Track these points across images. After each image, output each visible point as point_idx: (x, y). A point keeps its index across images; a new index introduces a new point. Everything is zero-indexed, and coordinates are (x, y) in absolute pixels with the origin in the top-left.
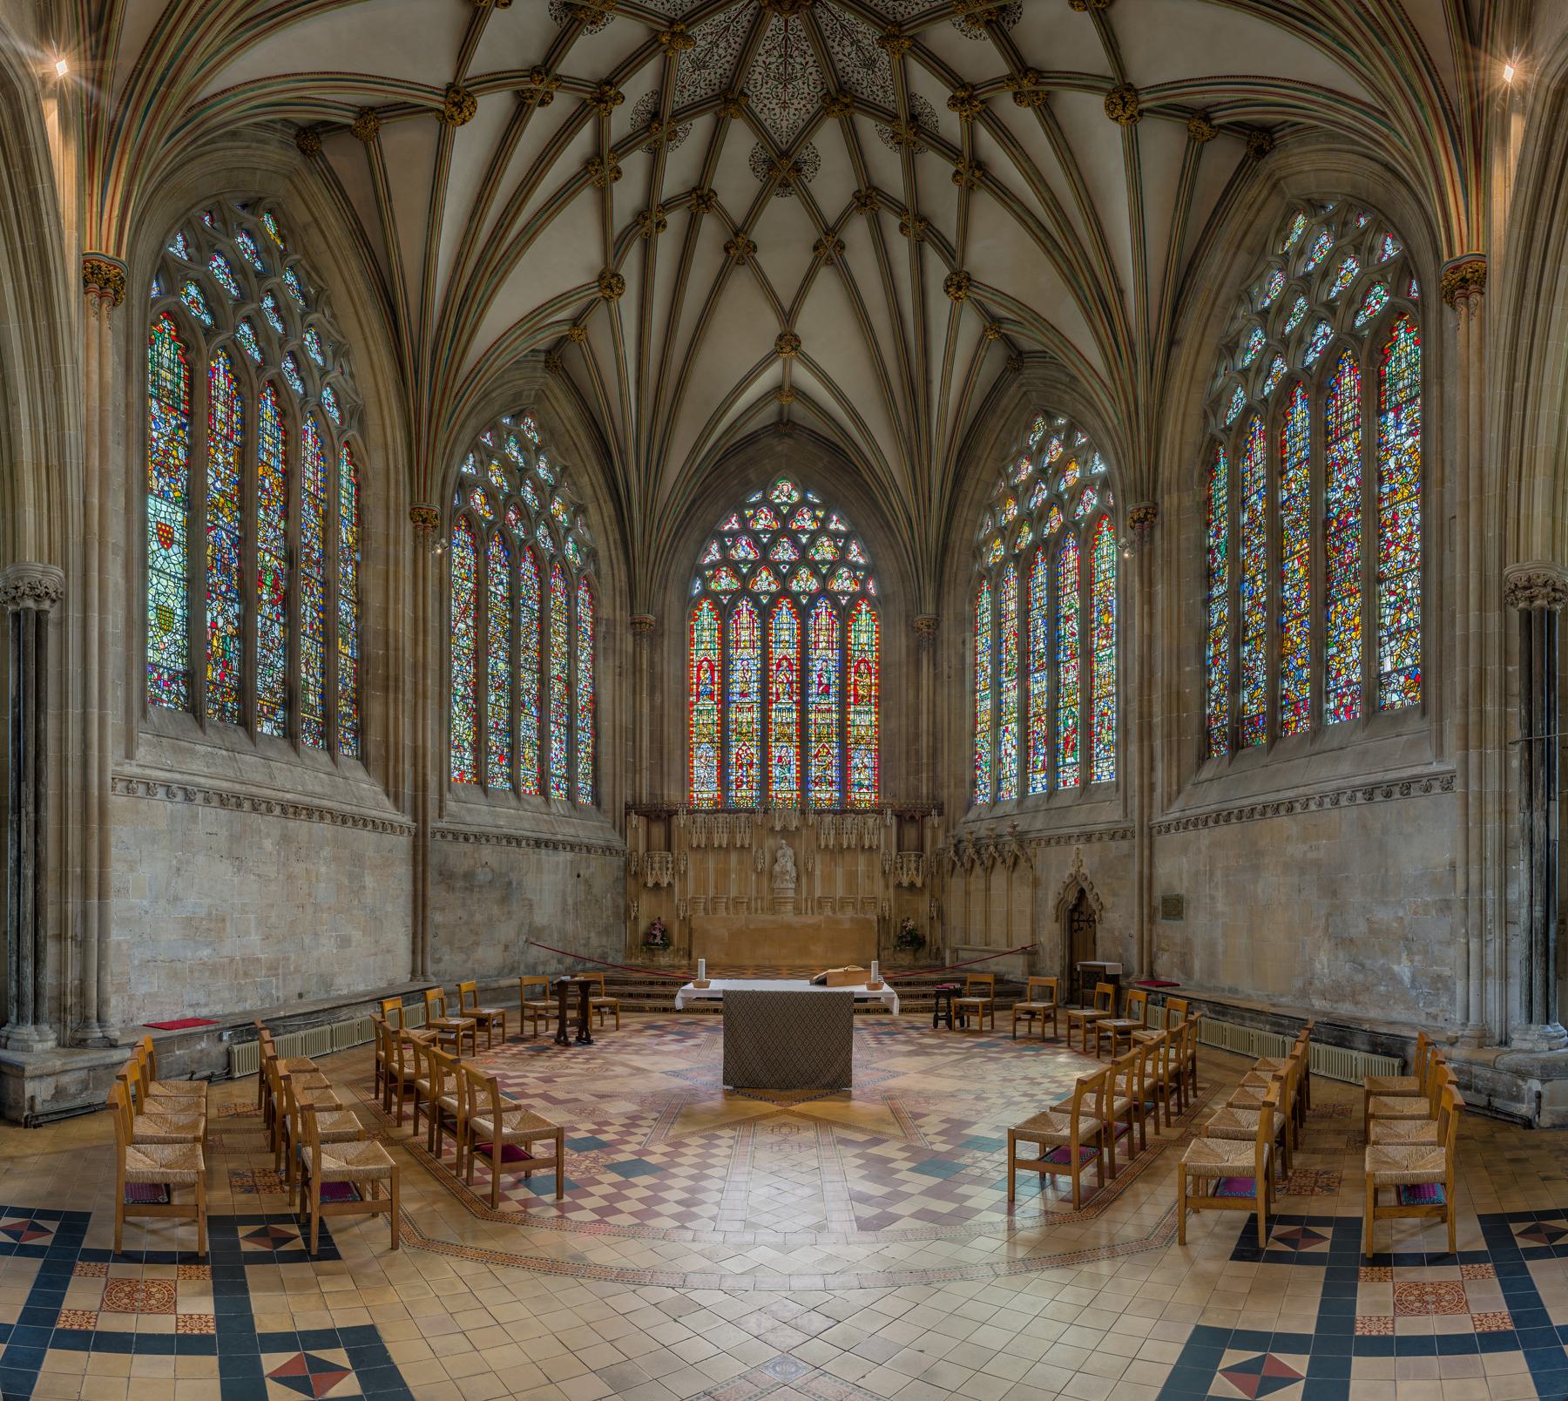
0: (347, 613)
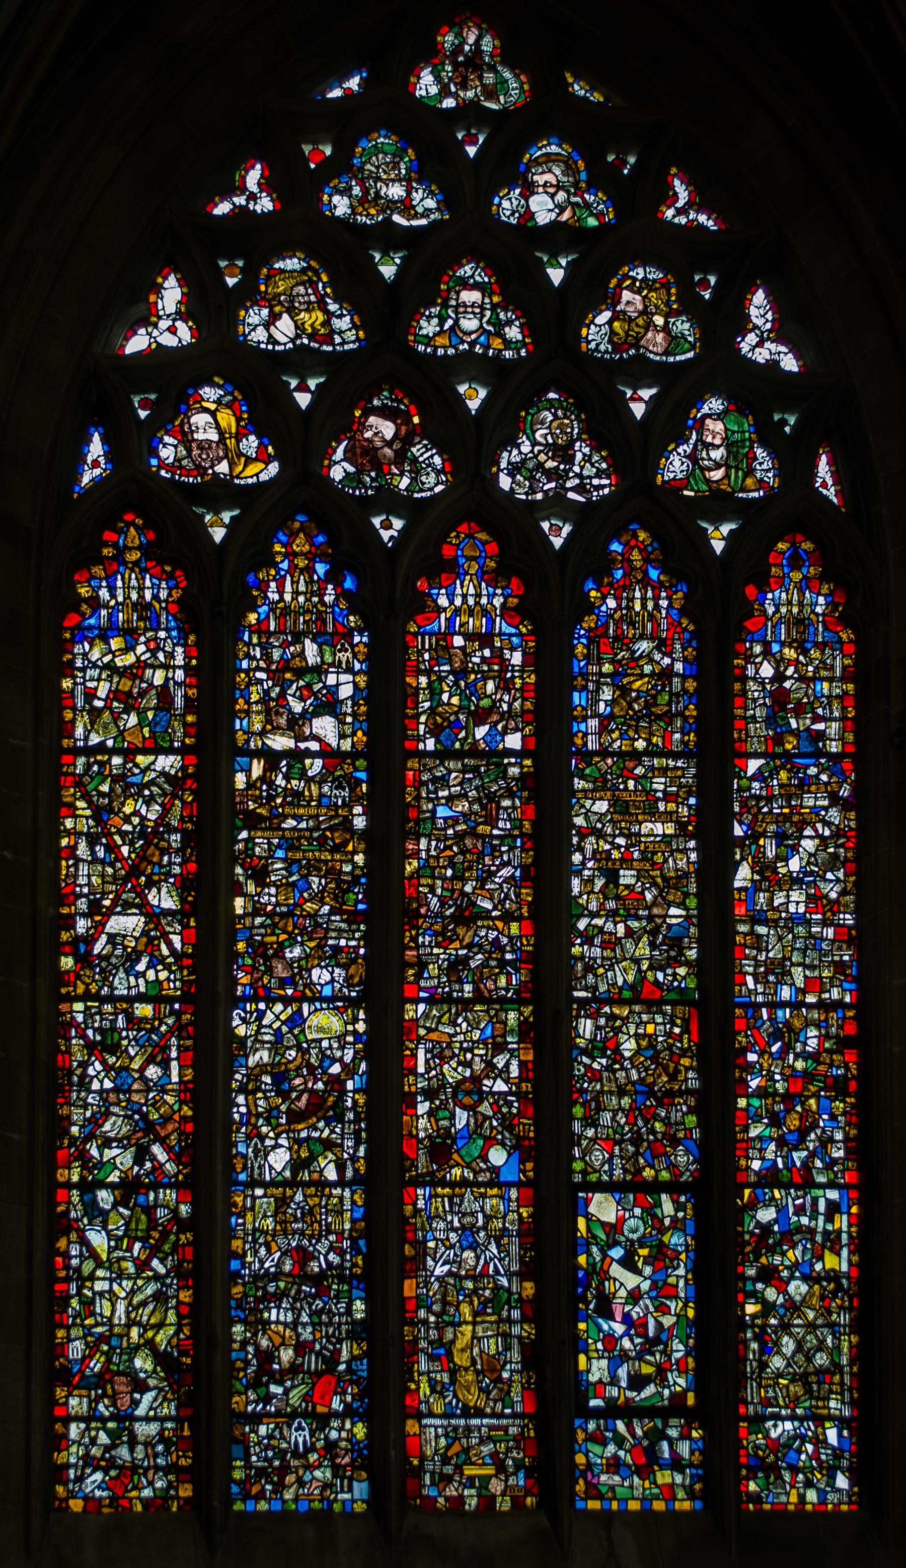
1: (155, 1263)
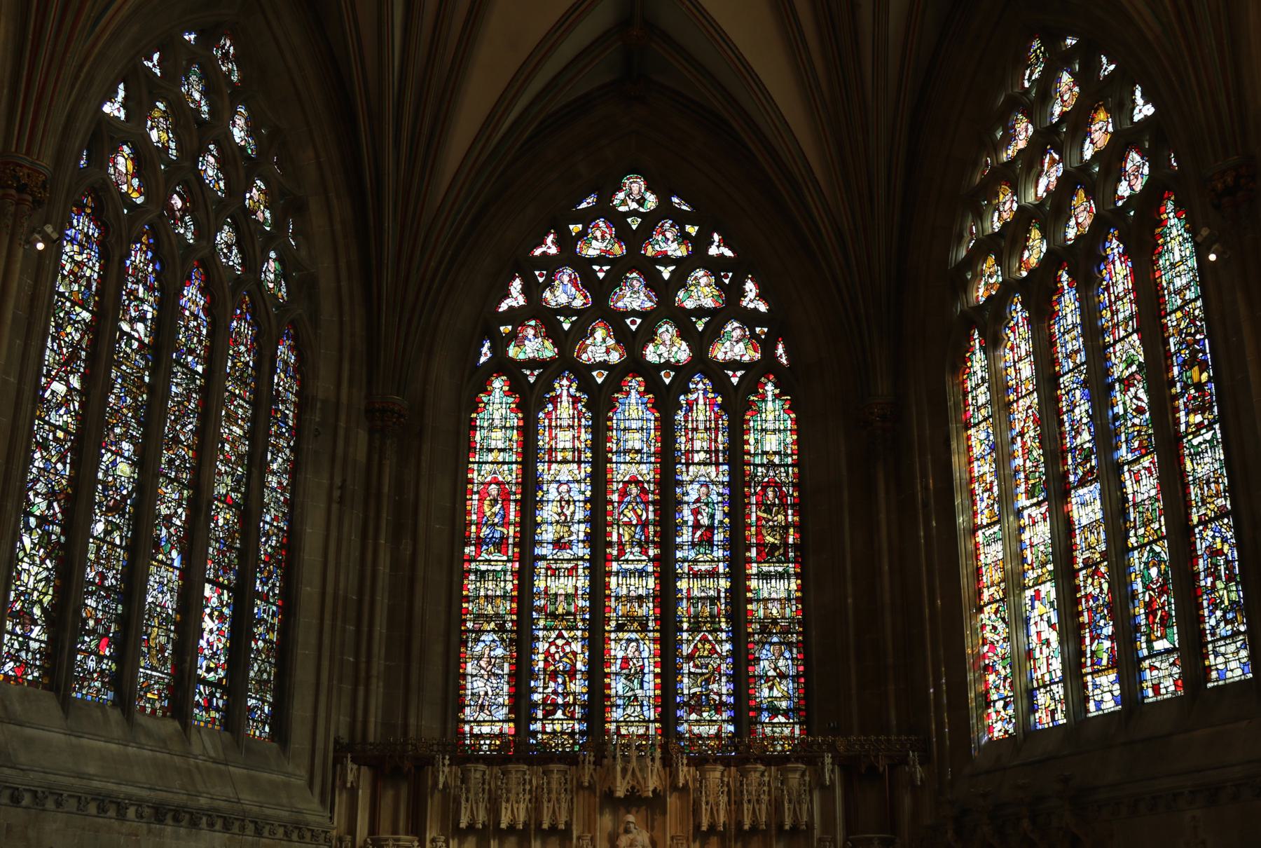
1: (48, 561)
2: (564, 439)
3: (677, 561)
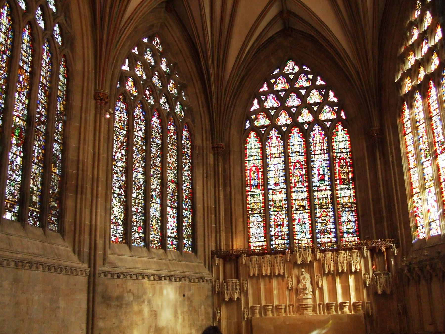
0: (57, 150)
2: (275, 150)
3: (313, 186)
